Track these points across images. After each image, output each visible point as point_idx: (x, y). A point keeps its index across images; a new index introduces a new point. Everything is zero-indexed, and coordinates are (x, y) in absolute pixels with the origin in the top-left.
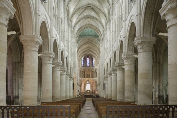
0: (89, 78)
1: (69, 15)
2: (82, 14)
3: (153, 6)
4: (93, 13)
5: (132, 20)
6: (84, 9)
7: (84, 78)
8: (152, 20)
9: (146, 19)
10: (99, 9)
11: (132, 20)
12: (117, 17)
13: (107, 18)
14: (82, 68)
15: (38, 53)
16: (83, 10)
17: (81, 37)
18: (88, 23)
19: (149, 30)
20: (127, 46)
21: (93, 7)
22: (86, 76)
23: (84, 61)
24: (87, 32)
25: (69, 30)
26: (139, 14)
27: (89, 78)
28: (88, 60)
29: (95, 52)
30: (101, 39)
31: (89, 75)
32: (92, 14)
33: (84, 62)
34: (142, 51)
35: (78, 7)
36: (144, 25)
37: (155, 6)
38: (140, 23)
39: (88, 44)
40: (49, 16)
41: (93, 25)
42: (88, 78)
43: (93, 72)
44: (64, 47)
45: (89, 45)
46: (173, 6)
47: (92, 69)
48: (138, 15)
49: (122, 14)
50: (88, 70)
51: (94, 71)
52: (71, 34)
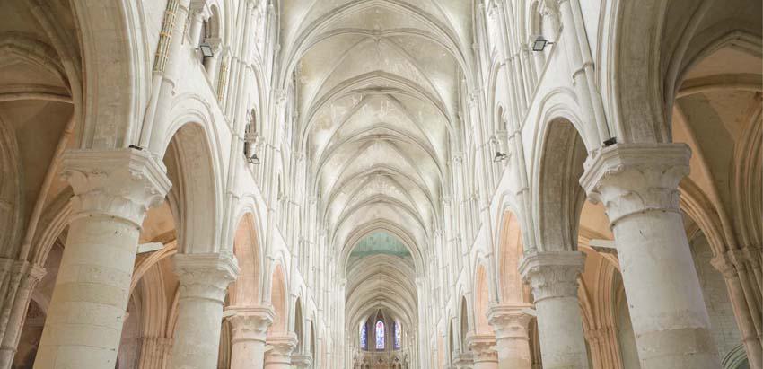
1: (324, 196)
2: (360, 193)
3: (561, 168)
4: (393, 187)
5: (505, 206)
6: (366, 178)
8: (562, 203)
9: (546, 201)
10: (408, 178)
12: (461, 199)
13: (435, 203)
15: (222, 307)
16: (362, 181)
17: (355, 258)
18: (378, 216)
19: (560, 233)
20: (498, 281)
21: (391, 172)
23: (366, 333)
24: (375, 243)
25: (323, 238)
28: (380, 329)
29: (400, 301)
30: (417, 261)
32: (390, 191)
33: (367, 335)
34: (545, 295)
35: (348, 173)
36: (542, 219)
37: (565, 166)
38: (531, 215)
39: (380, 278)
40: (263, 198)
41: (395, 225)
44: (304, 287)
45: (382, 281)
46: (615, 167)
47: (393, 358)
49: (476, 189)
50: (381, 361)
51: (400, 365)
52: (328, 248)
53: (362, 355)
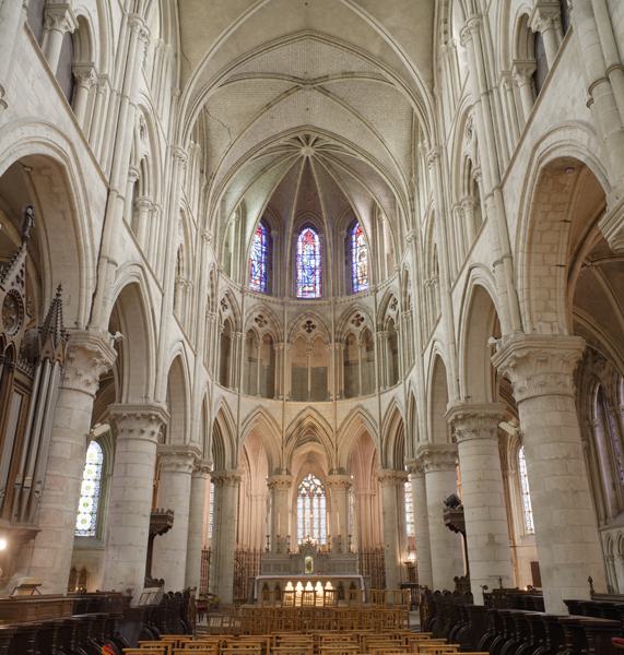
0: (321, 394)
7: (271, 393)
11: (473, 280)
14: (250, 301)
22: (286, 383)
26: (504, 257)
27: (320, 406)
28: (308, 250)
31: (321, 376)
42: (302, 400)
43: (358, 341)
47: (345, 317)
48: (607, 79)
50: (309, 326)
51: (367, 335)
53: (249, 305)
